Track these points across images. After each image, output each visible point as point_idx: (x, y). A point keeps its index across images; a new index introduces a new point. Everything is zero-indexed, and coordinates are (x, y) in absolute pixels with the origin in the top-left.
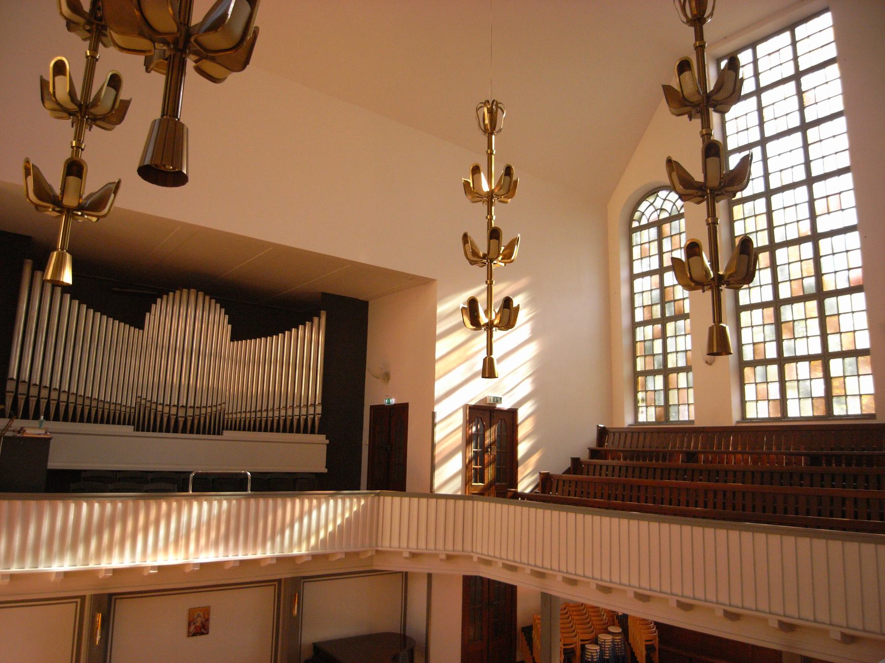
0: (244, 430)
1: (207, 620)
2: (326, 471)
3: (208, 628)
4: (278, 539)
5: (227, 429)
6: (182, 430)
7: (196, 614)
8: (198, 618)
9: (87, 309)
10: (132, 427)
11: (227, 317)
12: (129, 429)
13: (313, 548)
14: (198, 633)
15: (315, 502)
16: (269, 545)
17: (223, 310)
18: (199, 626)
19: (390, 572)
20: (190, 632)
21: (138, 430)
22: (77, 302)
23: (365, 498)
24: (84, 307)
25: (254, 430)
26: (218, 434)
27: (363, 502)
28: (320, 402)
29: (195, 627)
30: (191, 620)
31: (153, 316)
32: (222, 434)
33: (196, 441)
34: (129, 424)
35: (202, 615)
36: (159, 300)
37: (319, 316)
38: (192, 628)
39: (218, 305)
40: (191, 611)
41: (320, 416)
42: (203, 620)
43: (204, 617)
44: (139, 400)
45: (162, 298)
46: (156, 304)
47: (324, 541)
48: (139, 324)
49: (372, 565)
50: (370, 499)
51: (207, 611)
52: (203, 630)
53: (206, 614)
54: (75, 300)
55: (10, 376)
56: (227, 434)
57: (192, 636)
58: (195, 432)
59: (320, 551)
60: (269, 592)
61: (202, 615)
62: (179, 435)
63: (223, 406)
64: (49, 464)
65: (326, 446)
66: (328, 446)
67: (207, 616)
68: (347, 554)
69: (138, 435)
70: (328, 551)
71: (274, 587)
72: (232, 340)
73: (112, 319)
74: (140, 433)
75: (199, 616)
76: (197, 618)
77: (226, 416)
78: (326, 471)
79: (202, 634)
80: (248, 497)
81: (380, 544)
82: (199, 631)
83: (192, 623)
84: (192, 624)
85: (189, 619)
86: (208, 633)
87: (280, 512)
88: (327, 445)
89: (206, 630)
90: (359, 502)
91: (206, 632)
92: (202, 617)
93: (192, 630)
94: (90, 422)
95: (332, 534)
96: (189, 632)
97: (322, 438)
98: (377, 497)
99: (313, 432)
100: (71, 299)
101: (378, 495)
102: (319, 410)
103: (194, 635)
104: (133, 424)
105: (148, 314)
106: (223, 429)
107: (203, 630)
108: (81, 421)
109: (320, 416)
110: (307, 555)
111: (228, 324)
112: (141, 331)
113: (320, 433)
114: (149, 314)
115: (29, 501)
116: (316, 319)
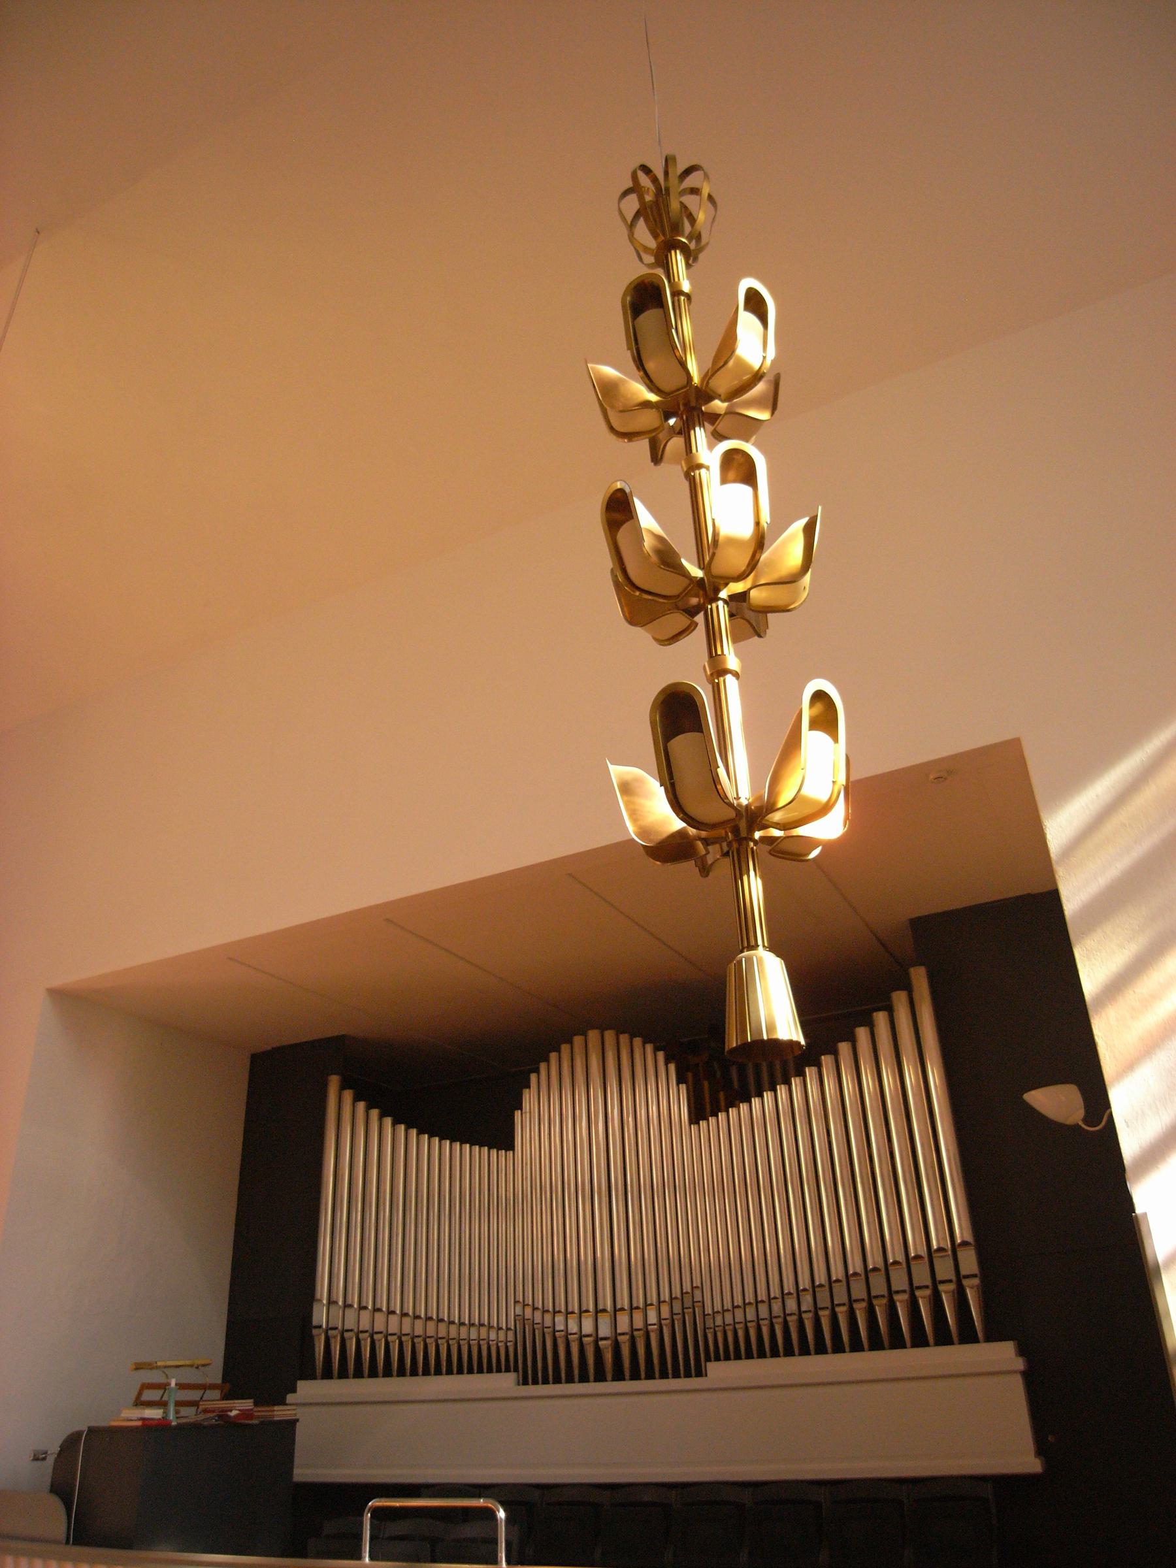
5: (718, 1359)
9: (418, 1135)
11: (672, 1067)
12: (506, 1382)
17: (661, 1055)
21: (525, 1383)
22: (403, 1127)
24: (414, 1132)
25: (789, 1352)
26: (700, 1373)
28: (969, 1238)
32: (706, 1376)
34: (508, 1370)
36: (533, 1077)
37: (907, 986)
39: (649, 1048)
41: (976, 1281)
44: (519, 1310)
46: (529, 1087)
48: (503, 1140)
54: (399, 1125)
55: (318, 1296)
56: (717, 1371)
58: (657, 1374)
63: (697, 1293)
64: (296, 1471)
73: (468, 1145)
74: (531, 1390)
77: (710, 1323)
94: (347, 1377)
99: (968, 1336)
100: (394, 1124)
102: (969, 1262)
104: (516, 1370)
105: (518, 1114)
106: (708, 1359)
108: (358, 1374)
111: (678, 1084)
116: (900, 999)
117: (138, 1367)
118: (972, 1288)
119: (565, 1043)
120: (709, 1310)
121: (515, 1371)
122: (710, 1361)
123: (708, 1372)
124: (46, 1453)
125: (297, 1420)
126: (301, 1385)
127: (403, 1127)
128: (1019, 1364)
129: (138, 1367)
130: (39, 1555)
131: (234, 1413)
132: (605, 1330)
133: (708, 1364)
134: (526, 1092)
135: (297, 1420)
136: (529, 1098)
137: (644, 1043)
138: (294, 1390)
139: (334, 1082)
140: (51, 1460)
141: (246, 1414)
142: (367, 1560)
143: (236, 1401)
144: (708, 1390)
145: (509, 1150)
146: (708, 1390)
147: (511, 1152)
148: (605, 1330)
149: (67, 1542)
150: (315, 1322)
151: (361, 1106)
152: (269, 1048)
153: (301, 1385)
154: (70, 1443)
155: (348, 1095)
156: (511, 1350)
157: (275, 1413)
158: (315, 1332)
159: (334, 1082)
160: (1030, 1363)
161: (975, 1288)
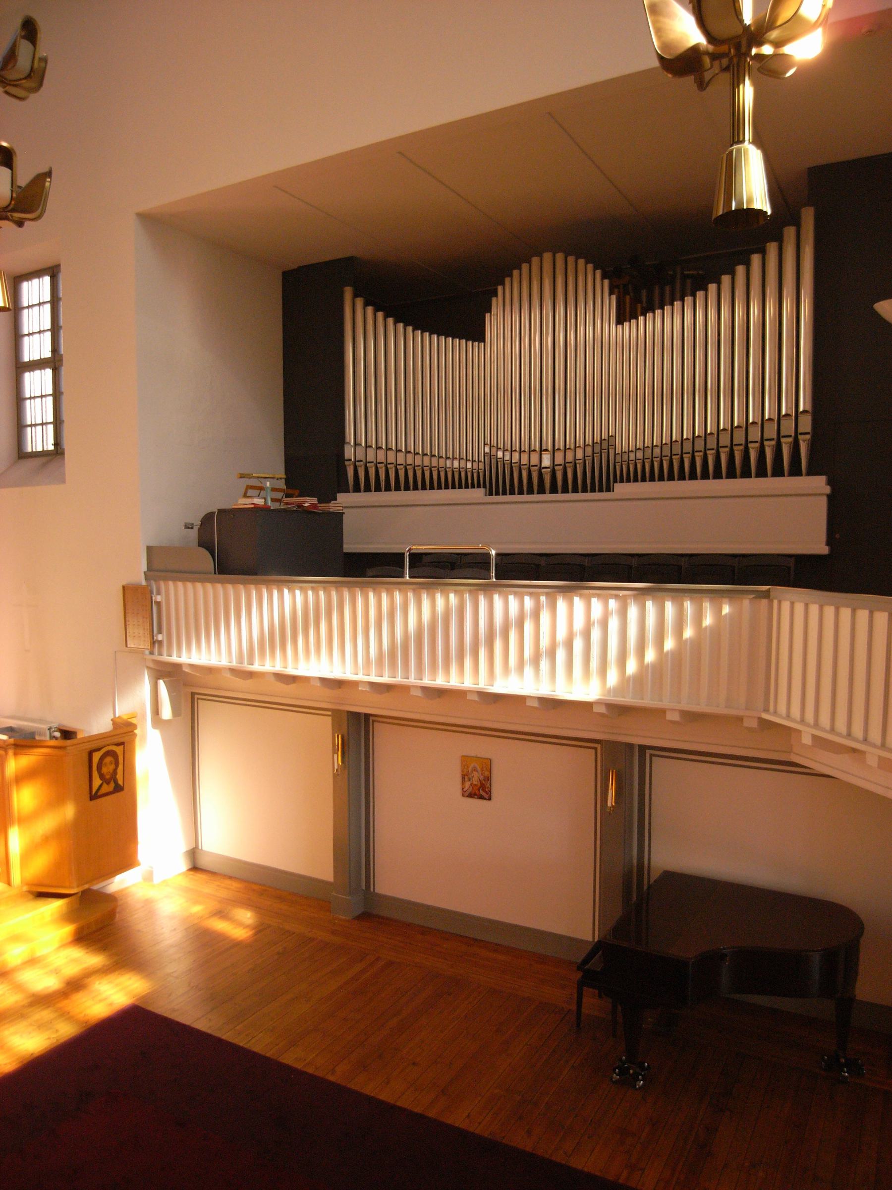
0: (652, 479)
1: (488, 779)
2: (824, 550)
3: (490, 791)
4: (544, 664)
5: (622, 481)
6: (599, 489)
7: (472, 765)
8: (474, 772)
10: (482, 490)
11: (606, 282)
12: (478, 494)
13: (616, 691)
14: (475, 794)
15: (613, 604)
16: (528, 670)
17: (598, 273)
18: (476, 785)
19: (812, 772)
20: (465, 790)
21: (491, 494)
23: (731, 600)
24: (410, 329)
25: (671, 478)
26: (609, 489)
27: (726, 609)
28: (809, 408)
29: (471, 785)
30: (464, 773)
31: (495, 317)
32: (613, 491)
33: (567, 504)
34: (479, 486)
35: (479, 769)
36: (500, 288)
38: (467, 784)
39: (590, 267)
40: (465, 760)
41: (808, 437)
42: (482, 778)
43: (482, 775)
44: (487, 450)
45: (503, 284)
46: (496, 296)
47: (639, 680)
48: (479, 336)
49: (790, 752)
50: (746, 603)
51: (487, 765)
52: (482, 792)
53: (484, 769)
55: (347, 440)
56: (621, 489)
57: (468, 796)
59: (628, 700)
60: (586, 758)
61: (479, 769)
62: (548, 497)
65: (824, 501)
66: (830, 498)
67: (487, 773)
68: (685, 714)
69: (523, 500)
70: (648, 701)
71: (654, 758)
72: (620, 321)
74: (495, 498)
75: (475, 770)
76: (472, 772)
77: (618, 459)
78: (824, 550)
79: (481, 797)
80: (488, 589)
81: (772, 708)
82: (477, 792)
83: (466, 777)
84: (466, 779)
85: (462, 771)
86: (490, 799)
87: (545, 617)
88: (828, 496)
89: (487, 794)
90: (720, 610)
91: (487, 798)
92: (480, 772)
93: (466, 788)
95: (658, 669)
96: (463, 789)
97: (819, 484)
98: (764, 602)
99: (796, 471)
100: (395, 323)
101: (767, 595)
102: (806, 424)
103: (471, 796)
104: (485, 487)
105: (487, 316)
106: (615, 481)
107: (482, 792)
109: (808, 437)
110: (598, 702)
111: (611, 293)
112: (483, 344)
113: (810, 473)
114: (489, 314)
115: (227, 584)
117: (242, 476)
118: (804, 441)
119: (524, 263)
120: (618, 450)
121: (483, 487)
122: (617, 482)
123: (614, 490)
124: (193, 524)
125: (344, 513)
126: (339, 496)
127: (402, 325)
128: (828, 490)
129: (242, 476)
130: (199, 581)
131: (307, 505)
132: (546, 461)
133: (615, 484)
134: (494, 300)
135: (344, 513)
136: (496, 304)
137: (586, 263)
138: (336, 499)
139: (348, 292)
140: (196, 528)
141: (313, 506)
142: (408, 578)
143: (307, 498)
144: (612, 500)
145: (482, 342)
146: (612, 500)
147: (483, 344)
148: (546, 461)
149: (215, 573)
150: (347, 456)
151: (370, 310)
152: (295, 266)
153: (339, 496)
154: (208, 519)
155: (359, 302)
156: (481, 475)
157: (331, 507)
158: (346, 463)
159: (348, 292)
160: (833, 489)
161: (806, 442)
